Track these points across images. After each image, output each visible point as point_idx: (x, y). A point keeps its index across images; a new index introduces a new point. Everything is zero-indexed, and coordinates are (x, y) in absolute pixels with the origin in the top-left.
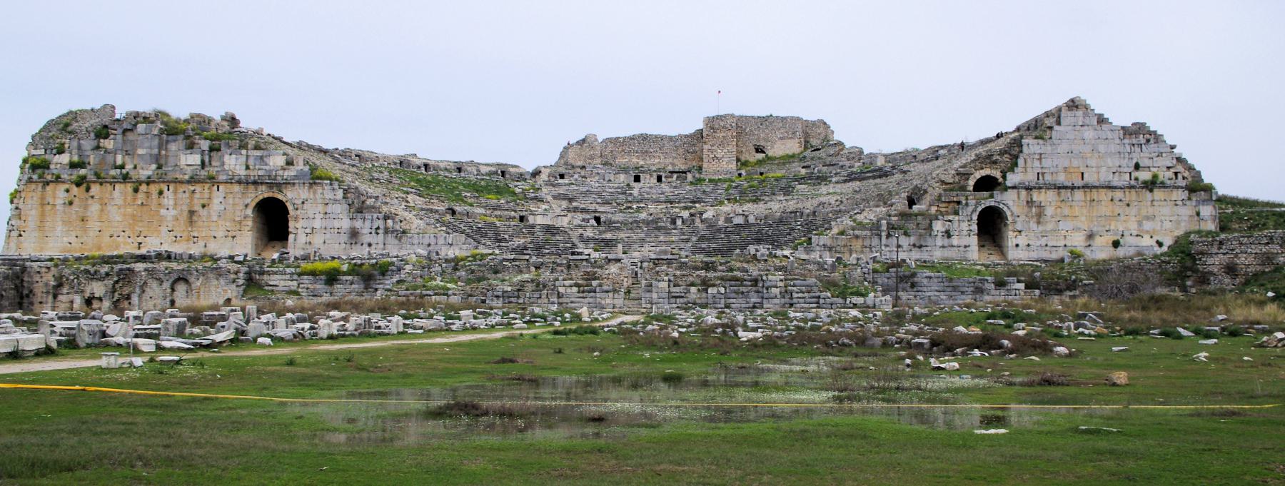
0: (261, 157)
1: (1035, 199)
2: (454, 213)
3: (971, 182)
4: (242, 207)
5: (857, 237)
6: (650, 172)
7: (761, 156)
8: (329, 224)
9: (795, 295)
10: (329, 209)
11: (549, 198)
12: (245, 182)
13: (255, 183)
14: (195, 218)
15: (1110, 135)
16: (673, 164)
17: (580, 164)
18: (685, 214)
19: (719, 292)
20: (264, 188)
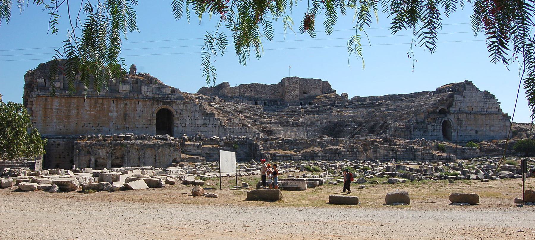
3: (438, 111)
7: (306, 95)
10: (193, 114)
14: (127, 118)
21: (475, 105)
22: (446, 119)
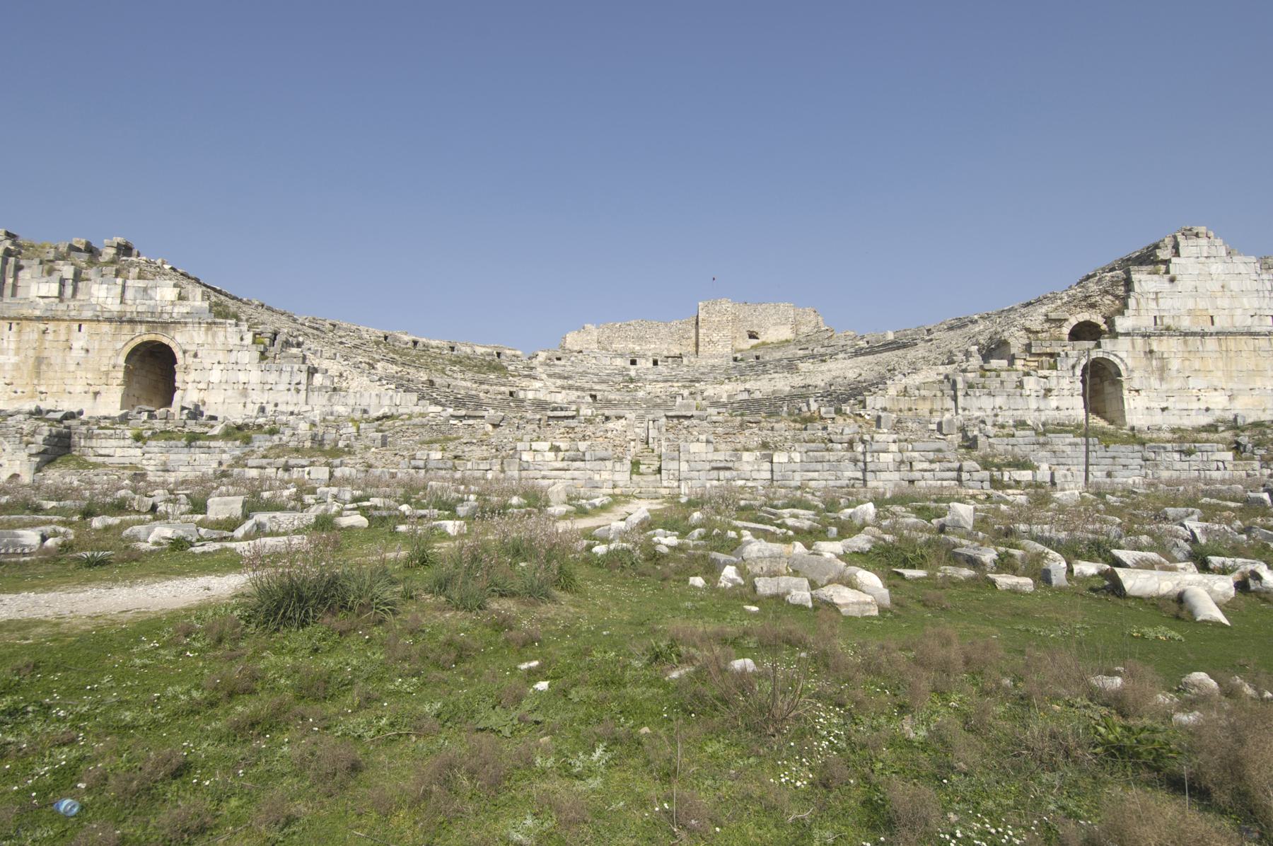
0: (145, 290)
1: (1155, 348)
2: (431, 383)
3: (1066, 330)
4: (110, 353)
5: (924, 398)
6: (644, 356)
7: (754, 342)
8: (232, 376)
9: (917, 466)
11: (544, 376)
12: (120, 320)
13: (131, 321)
14: (44, 367)
15: (1242, 268)
16: (668, 350)
17: (577, 348)
18: (686, 392)
19: (791, 460)
20: (143, 328)
21: (1223, 302)
22: (1096, 354)
